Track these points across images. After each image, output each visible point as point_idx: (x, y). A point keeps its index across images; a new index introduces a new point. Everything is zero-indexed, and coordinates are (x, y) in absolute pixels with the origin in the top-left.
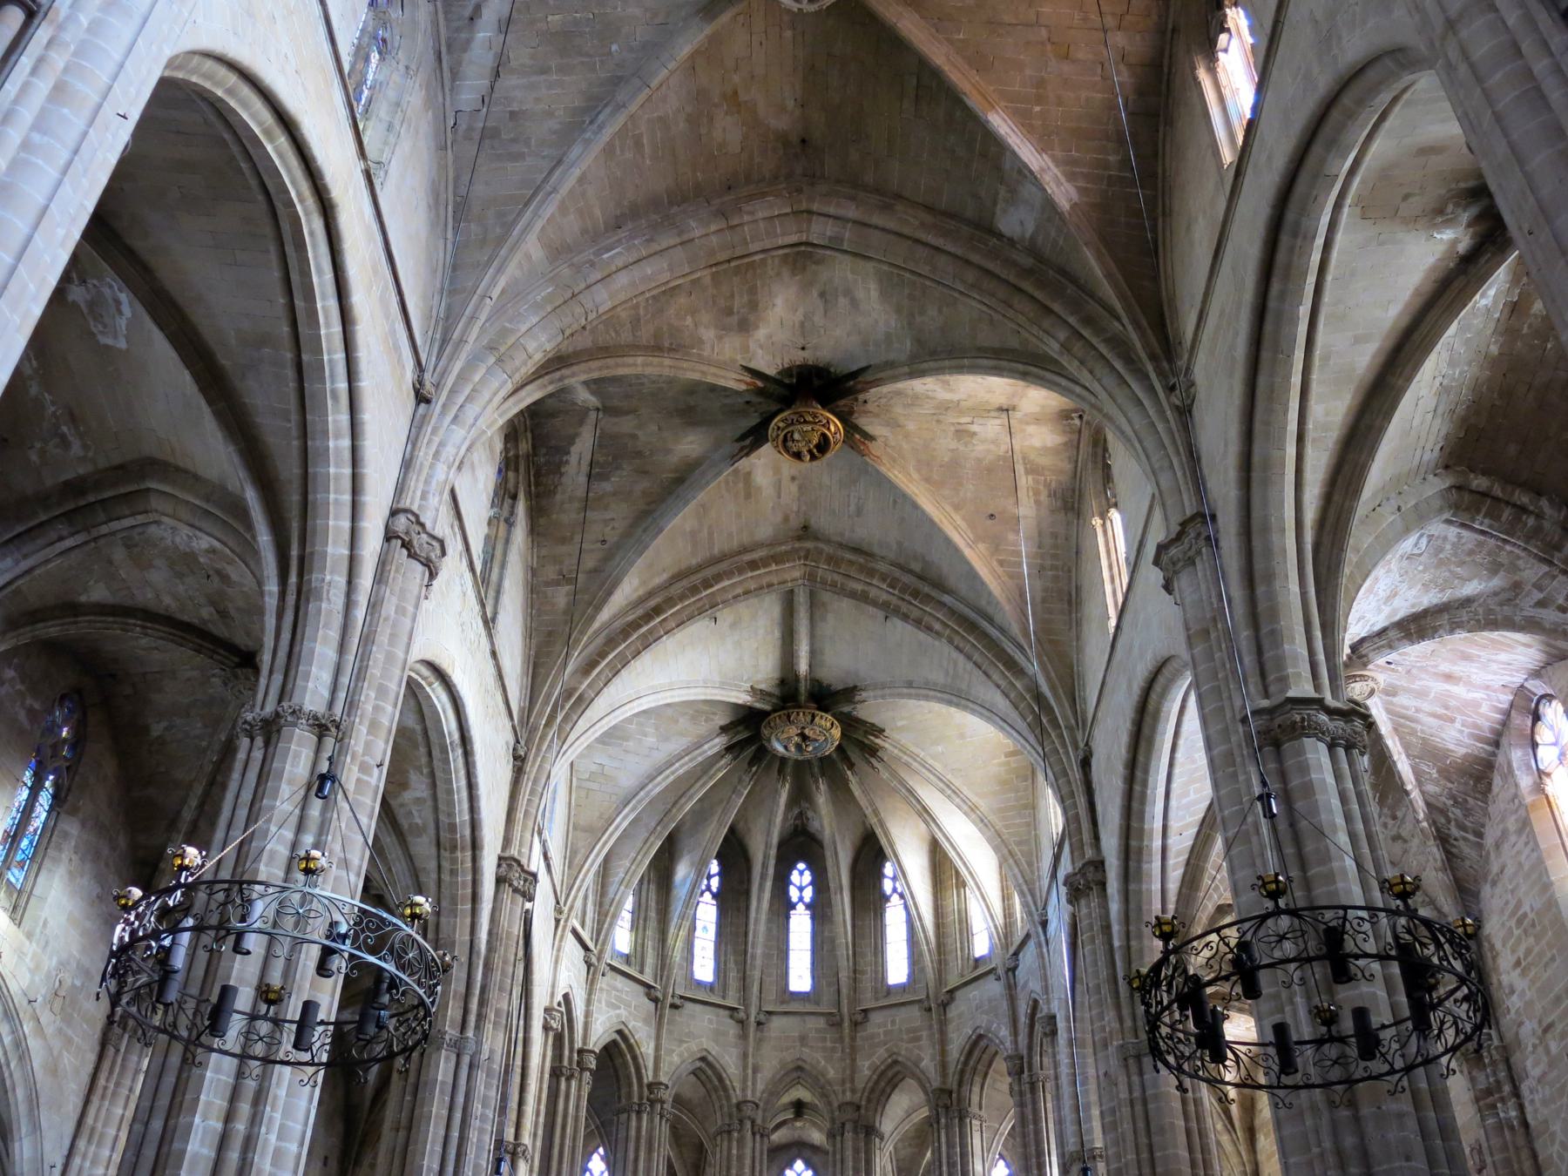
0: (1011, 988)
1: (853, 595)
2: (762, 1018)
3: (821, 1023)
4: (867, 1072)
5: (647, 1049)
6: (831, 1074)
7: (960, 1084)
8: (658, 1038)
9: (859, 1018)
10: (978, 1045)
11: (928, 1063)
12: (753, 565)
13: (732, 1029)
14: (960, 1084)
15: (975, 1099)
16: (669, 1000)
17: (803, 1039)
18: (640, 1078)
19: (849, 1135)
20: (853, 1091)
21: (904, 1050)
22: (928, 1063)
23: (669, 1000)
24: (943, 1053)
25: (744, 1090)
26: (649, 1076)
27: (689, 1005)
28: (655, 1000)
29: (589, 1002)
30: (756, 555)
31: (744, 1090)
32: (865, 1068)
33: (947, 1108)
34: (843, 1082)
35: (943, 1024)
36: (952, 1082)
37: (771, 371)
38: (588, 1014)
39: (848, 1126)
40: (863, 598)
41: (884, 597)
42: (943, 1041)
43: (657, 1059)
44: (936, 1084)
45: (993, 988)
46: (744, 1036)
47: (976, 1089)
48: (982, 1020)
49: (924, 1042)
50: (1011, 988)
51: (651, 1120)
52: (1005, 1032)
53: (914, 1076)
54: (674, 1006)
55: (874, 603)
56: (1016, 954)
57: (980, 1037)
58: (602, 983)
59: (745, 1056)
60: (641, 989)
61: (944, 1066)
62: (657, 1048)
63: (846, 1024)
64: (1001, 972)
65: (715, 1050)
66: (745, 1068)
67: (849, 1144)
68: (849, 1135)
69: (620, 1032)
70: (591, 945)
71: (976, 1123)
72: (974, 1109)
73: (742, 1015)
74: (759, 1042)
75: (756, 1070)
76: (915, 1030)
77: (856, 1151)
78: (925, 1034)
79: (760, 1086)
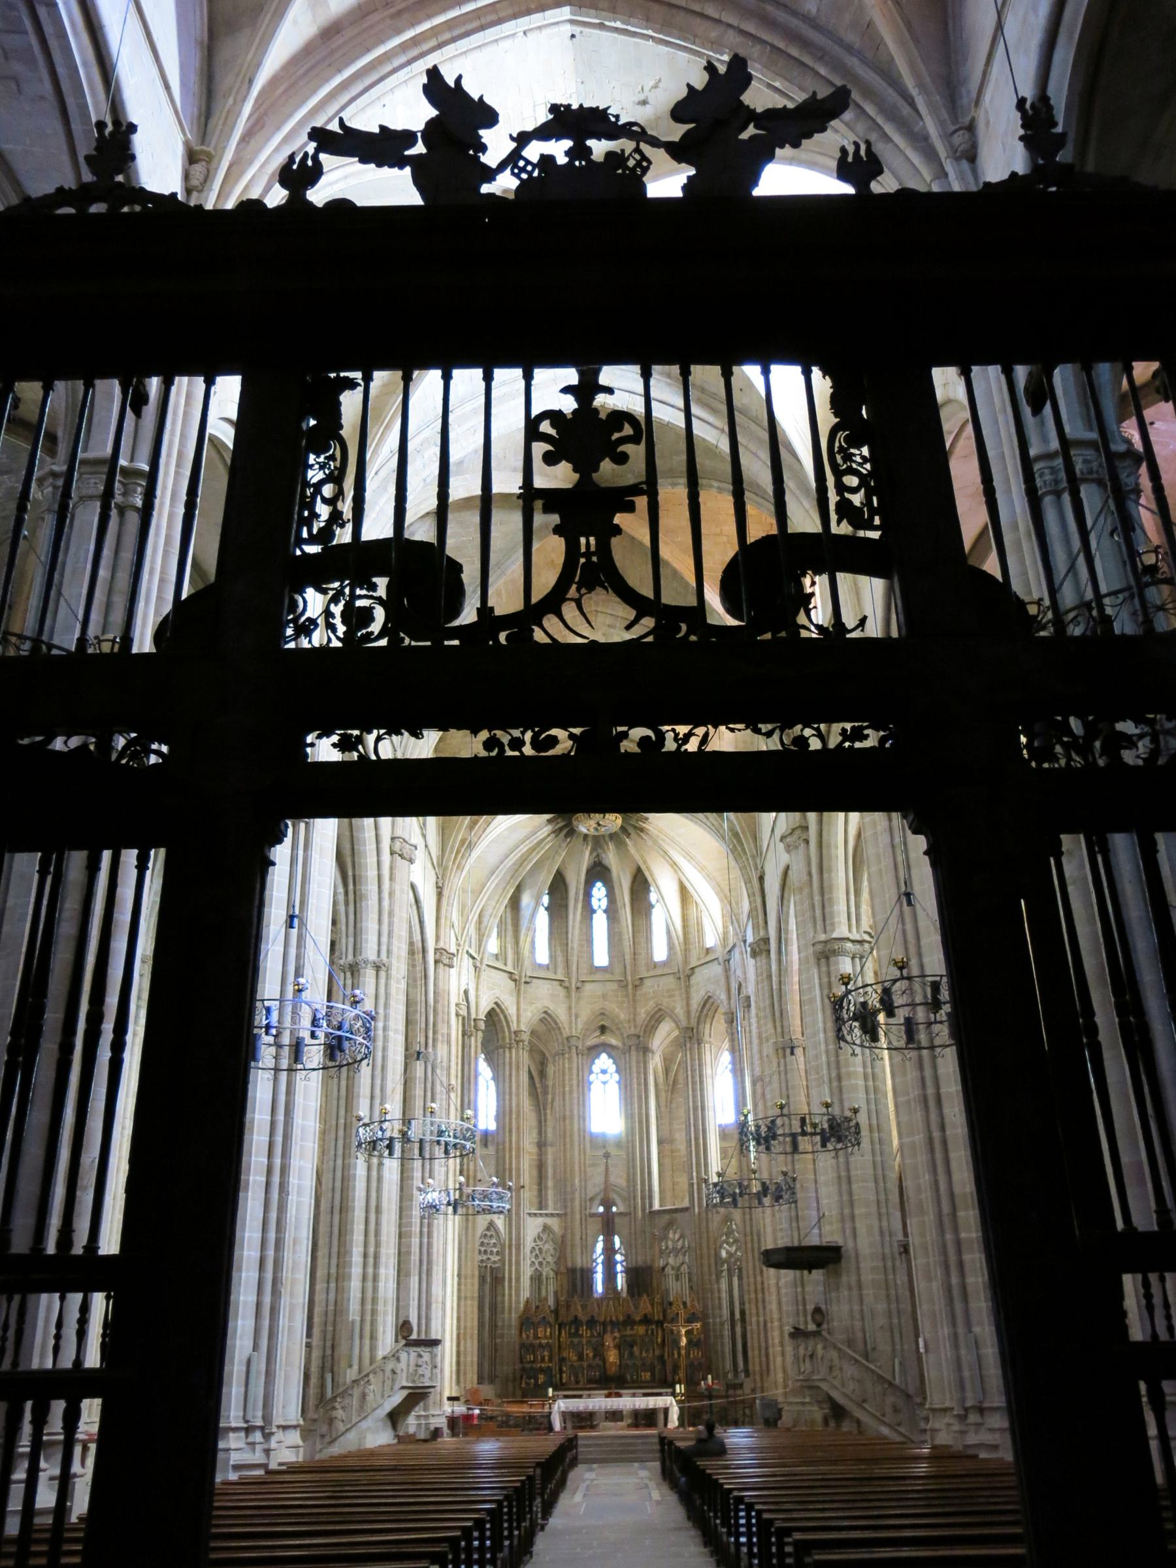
0: (727, 971)
2: (579, 985)
3: (615, 986)
4: (643, 1016)
5: (512, 1010)
6: (622, 1016)
7: (698, 1023)
8: (518, 1003)
9: (637, 983)
10: (708, 1003)
11: (679, 1011)
13: (561, 992)
14: (698, 1023)
15: (707, 1032)
16: (523, 980)
17: (604, 996)
19: (634, 1053)
20: (635, 1027)
21: (665, 1002)
22: (679, 1011)
23: (523, 980)
24: (688, 1005)
25: (570, 1028)
26: (514, 1027)
27: (535, 980)
28: (515, 980)
29: (477, 989)
31: (570, 1028)
32: (643, 1013)
33: (690, 1038)
34: (629, 1021)
35: (688, 987)
36: (693, 1023)
38: (477, 997)
39: (633, 1048)
42: (688, 999)
43: (518, 1016)
44: (684, 1023)
45: (717, 969)
46: (569, 996)
47: (707, 1026)
48: (711, 988)
49: (677, 998)
50: (727, 971)
51: (517, 1053)
52: (723, 996)
53: (671, 1017)
54: (526, 983)
56: (730, 951)
57: (709, 997)
58: (484, 975)
59: (570, 1008)
60: (506, 975)
61: (688, 1012)
62: (518, 1009)
63: (630, 987)
64: (721, 960)
65: (552, 1006)
66: (570, 1016)
67: (634, 1058)
68: (634, 1053)
69: (496, 1003)
70: (475, 955)
71: (707, 1046)
72: (706, 1038)
73: (567, 984)
74: (578, 999)
75: (577, 1016)
76: (668, 991)
77: (638, 1062)
78: (677, 993)
79: (580, 1026)
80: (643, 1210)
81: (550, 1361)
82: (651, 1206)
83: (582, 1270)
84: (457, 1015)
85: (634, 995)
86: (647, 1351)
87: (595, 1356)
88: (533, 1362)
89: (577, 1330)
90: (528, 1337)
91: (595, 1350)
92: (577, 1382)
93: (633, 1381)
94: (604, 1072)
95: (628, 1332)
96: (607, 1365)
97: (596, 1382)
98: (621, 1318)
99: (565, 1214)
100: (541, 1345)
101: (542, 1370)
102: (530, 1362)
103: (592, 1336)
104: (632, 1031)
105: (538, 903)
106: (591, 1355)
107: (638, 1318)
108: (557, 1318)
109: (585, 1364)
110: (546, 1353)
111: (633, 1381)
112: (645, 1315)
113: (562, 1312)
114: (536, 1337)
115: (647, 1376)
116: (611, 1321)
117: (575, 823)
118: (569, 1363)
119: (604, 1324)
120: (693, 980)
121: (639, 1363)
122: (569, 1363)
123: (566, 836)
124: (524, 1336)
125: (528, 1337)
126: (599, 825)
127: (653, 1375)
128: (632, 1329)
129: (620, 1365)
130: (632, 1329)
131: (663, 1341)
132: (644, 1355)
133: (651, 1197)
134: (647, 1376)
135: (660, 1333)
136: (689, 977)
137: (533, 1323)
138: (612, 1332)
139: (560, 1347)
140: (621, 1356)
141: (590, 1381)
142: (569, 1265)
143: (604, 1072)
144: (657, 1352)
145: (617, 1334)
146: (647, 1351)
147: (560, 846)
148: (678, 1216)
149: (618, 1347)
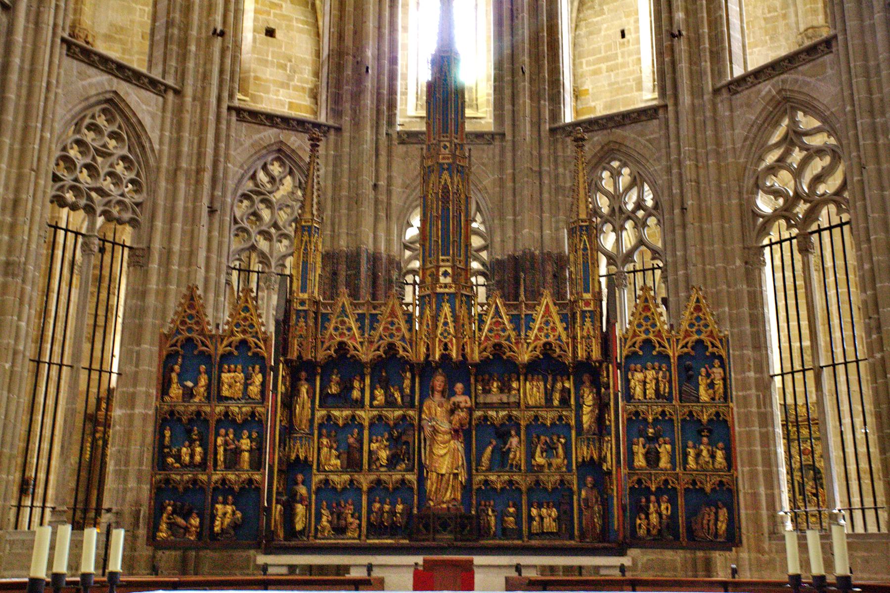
80: (537, 124)
81: (257, 464)
82: (555, 114)
83: (375, 259)
86: (550, 449)
87: (393, 462)
88: (203, 465)
89: (347, 388)
90: (189, 394)
91: (394, 442)
92: (340, 530)
93: (505, 532)
95: (495, 397)
96: (431, 485)
97: (392, 530)
98: (476, 356)
99: (338, 130)
100: (227, 420)
101: (224, 490)
102: (192, 465)
103: (390, 403)
106: (384, 454)
107: (525, 357)
108: (283, 346)
109: (365, 481)
110: (245, 444)
111: (505, 532)
112: (547, 346)
113: (301, 327)
114: (214, 394)
115: (548, 518)
116: (445, 357)
118: (317, 478)
119: (425, 370)
121: (523, 481)
122: (317, 478)
124: (175, 391)
125: (189, 394)
127: (565, 518)
128: (505, 388)
129: (467, 488)
130: (505, 388)
131: (600, 420)
132: (539, 460)
133: (556, 99)
134: (548, 518)
135: (589, 399)
137: (206, 358)
138: (447, 392)
139: (289, 431)
140: (471, 461)
141: (375, 529)
142: (343, 243)
144: (583, 452)
145: (462, 399)
146: (550, 449)
148: (628, 133)
149: (461, 432)
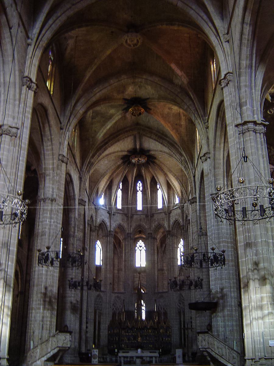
1: (148, 137)
5: (108, 224)
7: (172, 229)
11: (166, 225)
12: (127, 131)
18: (107, 230)
20: (151, 230)
26: (109, 229)
29: (96, 216)
30: (127, 129)
35: (169, 217)
36: (171, 229)
37: (129, 98)
38: (96, 219)
40: (150, 137)
41: (154, 138)
45: (179, 211)
48: (177, 217)
49: (165, 221)
55: (152, 139)
57: (176, 220)
61: (169, 226)
84: (88, 224)
85: (151, 220)
94: (141, 247)
104: (150, 232)
105: (118, 187)
117: (131, 159)
120: (171, 215)
123: (128, 165)
126: (139, 160)
136: (170, 213)
143: (141, 247)
147: (126, 168)
